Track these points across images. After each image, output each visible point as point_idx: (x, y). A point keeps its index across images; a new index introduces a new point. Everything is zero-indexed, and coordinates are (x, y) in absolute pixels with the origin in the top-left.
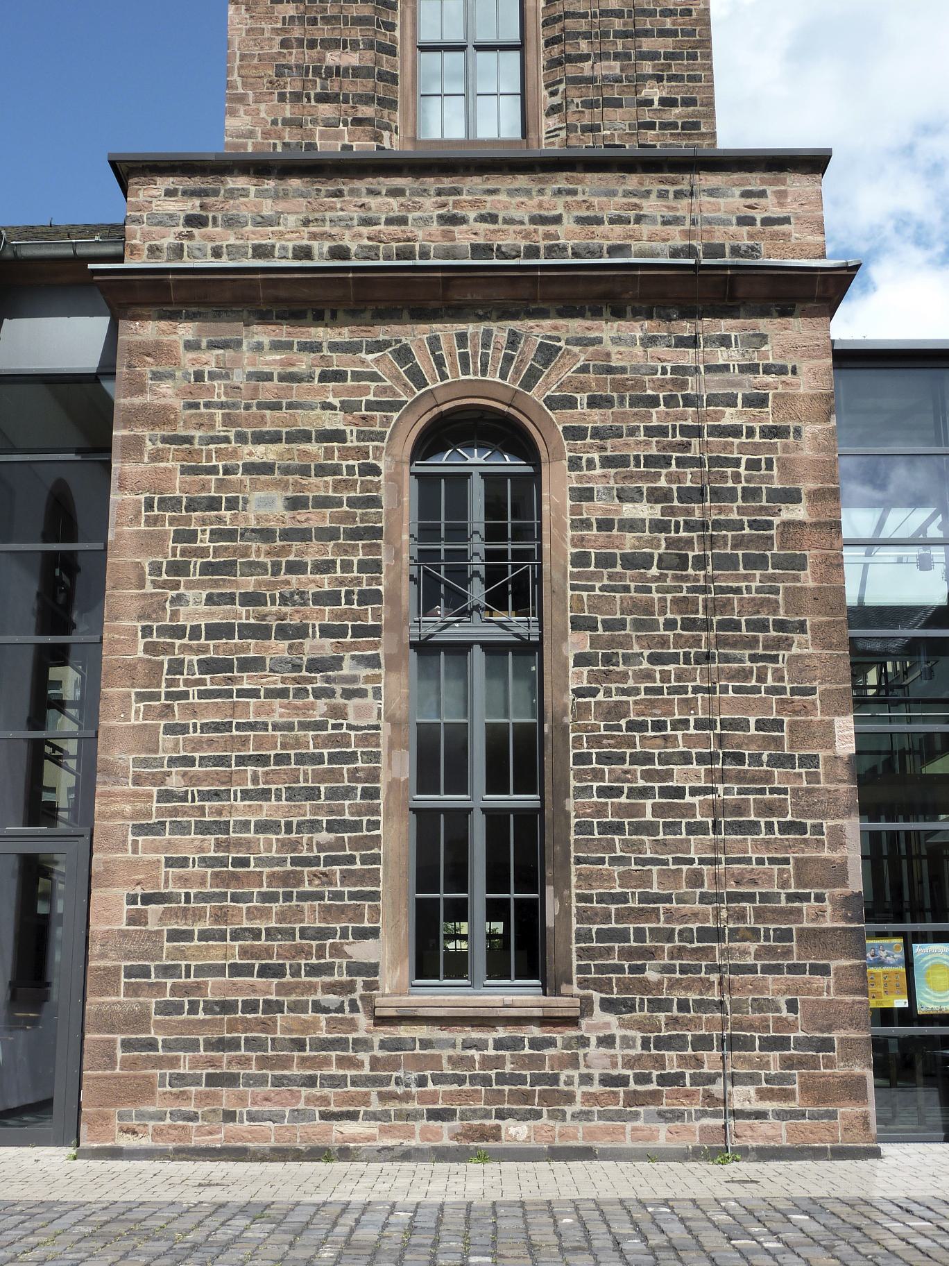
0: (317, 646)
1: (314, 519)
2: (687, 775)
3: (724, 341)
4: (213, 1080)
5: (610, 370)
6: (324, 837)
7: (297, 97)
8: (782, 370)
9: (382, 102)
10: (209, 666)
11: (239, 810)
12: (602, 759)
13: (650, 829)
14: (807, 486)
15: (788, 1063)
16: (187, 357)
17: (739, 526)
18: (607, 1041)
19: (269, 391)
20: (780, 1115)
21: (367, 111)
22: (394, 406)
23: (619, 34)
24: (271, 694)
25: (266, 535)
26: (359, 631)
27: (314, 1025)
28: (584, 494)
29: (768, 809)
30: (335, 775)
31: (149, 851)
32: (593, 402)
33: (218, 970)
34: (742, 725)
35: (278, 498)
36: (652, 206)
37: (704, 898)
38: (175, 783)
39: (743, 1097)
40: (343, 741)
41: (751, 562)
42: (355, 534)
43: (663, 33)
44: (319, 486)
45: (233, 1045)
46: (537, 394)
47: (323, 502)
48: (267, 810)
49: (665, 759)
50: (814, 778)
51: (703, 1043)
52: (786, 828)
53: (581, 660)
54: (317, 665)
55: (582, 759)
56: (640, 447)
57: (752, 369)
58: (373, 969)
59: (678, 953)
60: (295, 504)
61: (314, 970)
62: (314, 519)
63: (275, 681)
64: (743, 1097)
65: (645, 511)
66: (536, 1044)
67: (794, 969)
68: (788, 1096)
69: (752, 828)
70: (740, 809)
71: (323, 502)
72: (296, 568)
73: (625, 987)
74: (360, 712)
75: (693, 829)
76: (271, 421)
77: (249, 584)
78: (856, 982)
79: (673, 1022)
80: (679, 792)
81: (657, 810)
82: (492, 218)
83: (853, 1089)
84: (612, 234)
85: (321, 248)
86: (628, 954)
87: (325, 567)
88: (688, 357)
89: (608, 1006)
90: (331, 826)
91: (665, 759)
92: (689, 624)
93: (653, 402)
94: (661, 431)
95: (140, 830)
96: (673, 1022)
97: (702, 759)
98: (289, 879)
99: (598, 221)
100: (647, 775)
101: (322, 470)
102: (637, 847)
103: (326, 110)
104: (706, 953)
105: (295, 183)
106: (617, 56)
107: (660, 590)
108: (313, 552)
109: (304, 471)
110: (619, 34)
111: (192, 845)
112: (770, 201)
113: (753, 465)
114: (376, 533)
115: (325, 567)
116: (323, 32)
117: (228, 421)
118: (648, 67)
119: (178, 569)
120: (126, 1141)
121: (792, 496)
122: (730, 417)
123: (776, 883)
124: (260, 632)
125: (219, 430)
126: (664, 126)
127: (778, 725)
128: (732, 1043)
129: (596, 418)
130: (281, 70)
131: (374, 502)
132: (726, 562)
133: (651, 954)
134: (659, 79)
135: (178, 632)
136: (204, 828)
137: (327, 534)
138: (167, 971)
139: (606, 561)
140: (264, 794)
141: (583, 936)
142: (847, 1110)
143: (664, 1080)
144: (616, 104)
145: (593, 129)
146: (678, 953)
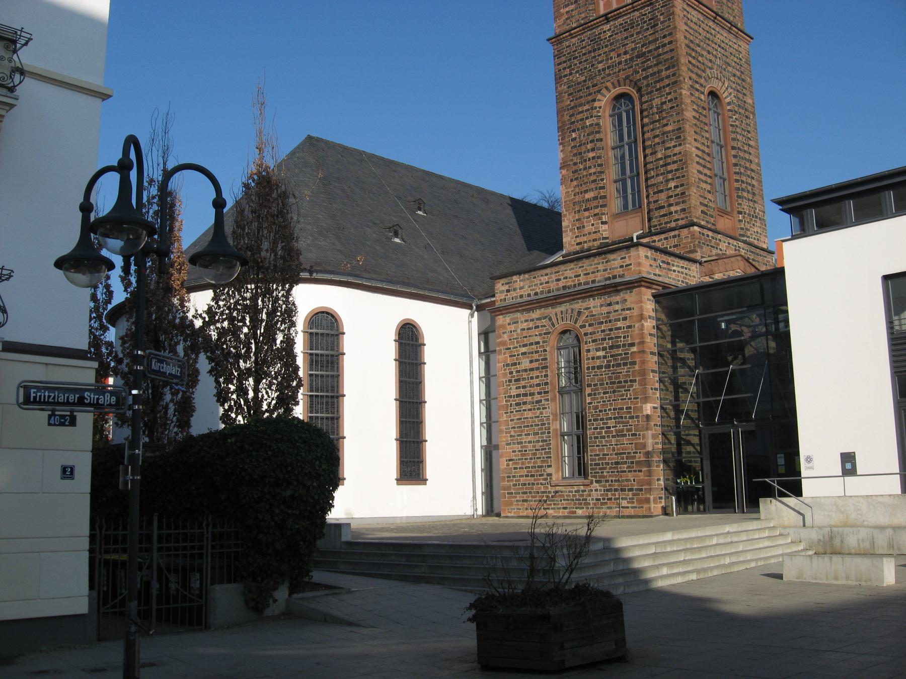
0: (537, 397)
1: (535, 365)
2: (611, 423)
3: (617, 303)
4: (523, 501)
5: (593, 316)
6: (541, 444)
7: (579, 211)
8: (629, 309)
9: (601, 206)
10: (518, 404)
11: (525, 439)
12: (594, 420)
13: (603, 437)
14: (637, 341)
15: (634, 495)
16: (508, 327)
17: (621, 355)
18: (596, 490)
19: (525, 333)
20: (632, 507)
21: (597, 211)
22: (549, 333)
23: (662, 166)
24: (530, 410)
25: (526, 370)
26: (545, 392)
27: (540, 488)
28: (588, 351)
29: (629, 430)
30: (541, 429)
31: (508, 449)
32: (590, 325)
33: (522, 476)
34: (622, 409)
35: (528, 360)
36: (601, 267)
37: (616, 454)
38: (512, 433)
39: (624, 503)
40: (543, 420)
41: (625, 364)
42: (543, 368)
43: (674, 162)
44: (536, 356)
45: (526, 493)
46: (578, 325)
47: (537, 360)
48: (530, 438)
49: (607, 419)
50: (638, 421)
51: (616, 490)
52: (633, 435)
53: (589, 395)
54: (538, 402)
55: (590, 420)
56: (600, 336)
57: (623, 310)
58: (550, 475)
59: (610, 468)
60: (531, 362)
61: (541, 475)
62: (535, 365)
63: (529, 407)
64: (624, 503)
65: (601, 353)
66: (583, 491)
67: (635, 471)
68: (633, 503)
70: (622, 431)
71: (537, 360)
72: (532, 378)
73: (600, 477)
74: (546, 413)
75: (613, 436)
76: (526, 341)
77: (523, 383)
78: (647, 474)
79: (610, 485)
80: (609, 428)
82: (566, 278)
84: (591, 277)
85: (532, 293)
86: (600, 469)
87: (537, 377)
88: (611, 308)
89: (596, 482)
90: (543, 441)
91: (607, 419)
92: (611, 383)
93: (602, 323)
94: (603, 331)
95: (507, 444)
96: (610, 485)
97: (615, 418)
98: (535, 454)
99: (588, 274)
100: (603, 424)
101: (537, 352)
102: (601, 442)
103: (587, 214)
104: (617, 468)
105: (527, 276)
106: (662, 174)
107: (604, 374)
108: (535, 373)
109: (532, 353)
110: (662, 166)
111: (517, 447)
112: (627, 259)
113: (624, 337)
114: (547, 367)
115: (537, 377)
116: (584, 188)
117: (517, 342)
118: (670, 176)
119: (510, 381)
120: (509, 515)
121: (632, 345)
122: (619, 324)
123: (631, 449)
124: (525, 395)
125: (516, 345)
126: (676, 195)
127: (630, 408)
128: (622, 490)
129: (589, 329)
130: (574, 204)
131: (546, 359)
132: (619, 365)
133: (605, 469)
134: (673, 179)
135: (510, 397)
136: (518, 443)
137: (537, 369)
138: (514, 476)
139: (593, 368)
140: (529, 434)
141: (591, 465)
142: (645, 506)
143: (608, 499)
144: (661, 191)
145: (657, 201)
146: (610, 468)
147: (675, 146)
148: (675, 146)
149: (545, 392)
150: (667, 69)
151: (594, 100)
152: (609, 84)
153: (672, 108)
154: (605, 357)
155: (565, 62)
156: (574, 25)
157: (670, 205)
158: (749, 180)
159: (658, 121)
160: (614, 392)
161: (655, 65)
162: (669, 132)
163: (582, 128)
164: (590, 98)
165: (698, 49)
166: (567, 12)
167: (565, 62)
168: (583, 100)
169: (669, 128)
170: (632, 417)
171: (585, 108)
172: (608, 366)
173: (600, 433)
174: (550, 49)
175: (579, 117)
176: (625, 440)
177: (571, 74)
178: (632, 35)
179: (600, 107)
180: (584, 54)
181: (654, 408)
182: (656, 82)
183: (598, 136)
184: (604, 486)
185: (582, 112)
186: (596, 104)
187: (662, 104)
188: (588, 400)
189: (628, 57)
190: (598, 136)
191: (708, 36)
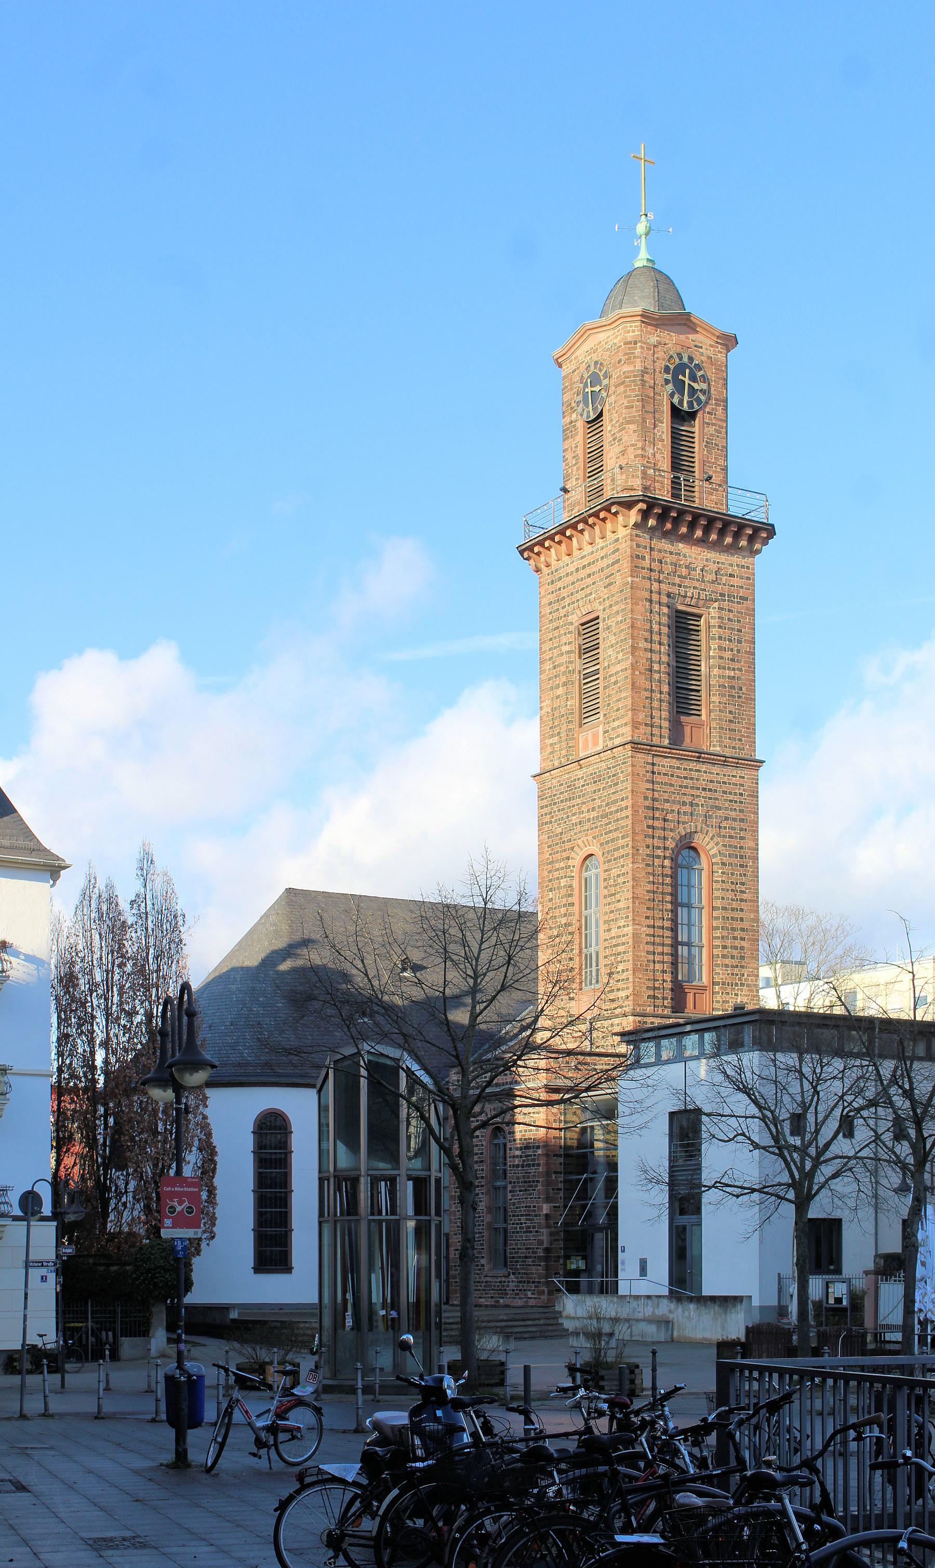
13: (518, 1232)
28: (511, 1149)
29: (534, 1227)
34: (530, 1207)
37: (527, 1249)
43: (623, 944)
52: (537, 1232)
53: (510, 1192)
58: (483, 1265)
69: (531, 1232)
81: (520, 1228)
83: (543, 1292)
89: (514, 1274)
97: (526, 1215)
110: (615, 946)
114: (482, 1162)
128: (529, 1282)
132: (529, 1165)
133: (517, 1262)
147: (624, 926)
148: (624, 926)
149: (482, 1186)
150: (623, 837)
151: (568, 858)
152: (580, 842)
153: (624, 883)
154: (521, 1157)
155: (546, 806)
156: (557, 764)
157: (618, 990)
158: (737, 943)
159: (614, 894)
160: (526, 1190)
161: (616, 830)
162: (620, 909)
163: (558, 888)
164: (565, 855)
165: (667, 806)
166: (551, 745)
167: (546, 806)
168: (558, 856)
169: (621, 905)
170: (536, 1216)
171: (562, 865)
172: (523, 1166)
173: (516, 1228)
174: (533, 785)
175: (556, 874)
176: (531, 1236)
177: (551, 822)
178: (599, 790)
179: (574, 866)
180: (562, 801)
181: (555, 1207)
182: (615, 850)
183: (570, 900)
184: (517, 1278)
185: (558, 870)
186: (570, 862)
187: (619, 876)
188: (509, 1196)
189: (595, 814)
190: (570, 900)
191: (685, 782)
